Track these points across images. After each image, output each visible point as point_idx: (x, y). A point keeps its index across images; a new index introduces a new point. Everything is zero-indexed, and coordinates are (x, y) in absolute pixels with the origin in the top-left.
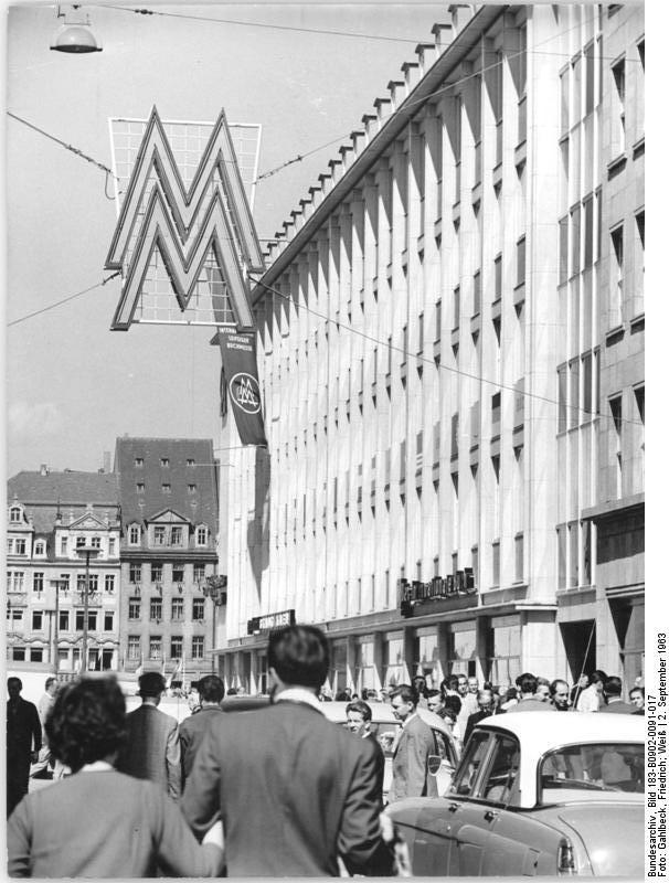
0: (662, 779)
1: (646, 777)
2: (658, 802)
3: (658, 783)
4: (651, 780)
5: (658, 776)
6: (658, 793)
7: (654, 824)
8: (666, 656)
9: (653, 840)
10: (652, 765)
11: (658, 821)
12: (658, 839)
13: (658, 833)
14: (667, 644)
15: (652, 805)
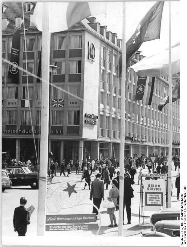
0: (185, 218)
1: (181, 217)
2: (184, 224)
3: (184, 219)
4: (182, 218)
5: (184, 217)
6: (184, 222)
7: (183, 230)
8: (186, 192)
9: (183, 235)
10: (182, 214)
11: (184, 230)
12: (184, 235)
13: (184, 233)
14: (186, 189)
15: (182, 225)
